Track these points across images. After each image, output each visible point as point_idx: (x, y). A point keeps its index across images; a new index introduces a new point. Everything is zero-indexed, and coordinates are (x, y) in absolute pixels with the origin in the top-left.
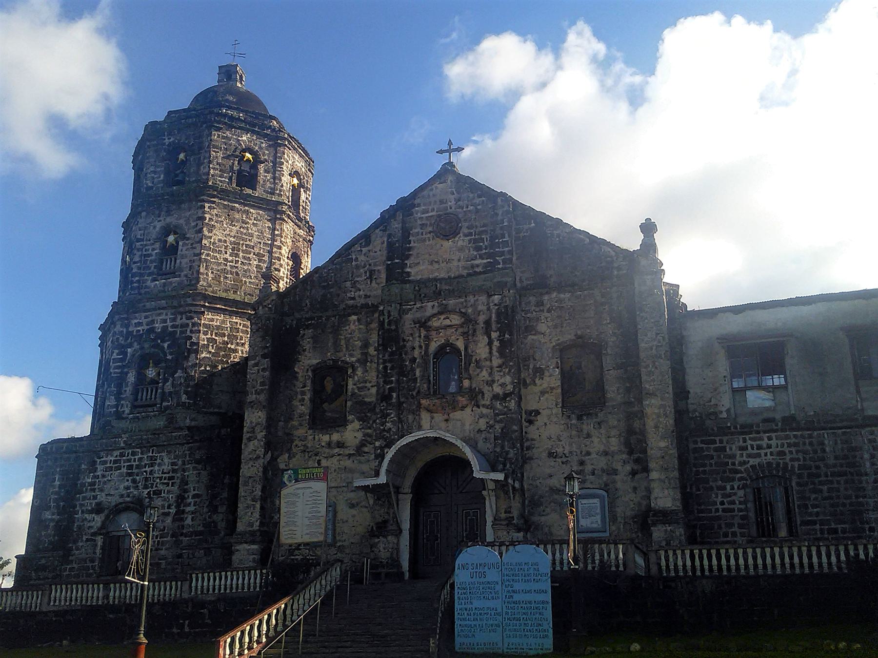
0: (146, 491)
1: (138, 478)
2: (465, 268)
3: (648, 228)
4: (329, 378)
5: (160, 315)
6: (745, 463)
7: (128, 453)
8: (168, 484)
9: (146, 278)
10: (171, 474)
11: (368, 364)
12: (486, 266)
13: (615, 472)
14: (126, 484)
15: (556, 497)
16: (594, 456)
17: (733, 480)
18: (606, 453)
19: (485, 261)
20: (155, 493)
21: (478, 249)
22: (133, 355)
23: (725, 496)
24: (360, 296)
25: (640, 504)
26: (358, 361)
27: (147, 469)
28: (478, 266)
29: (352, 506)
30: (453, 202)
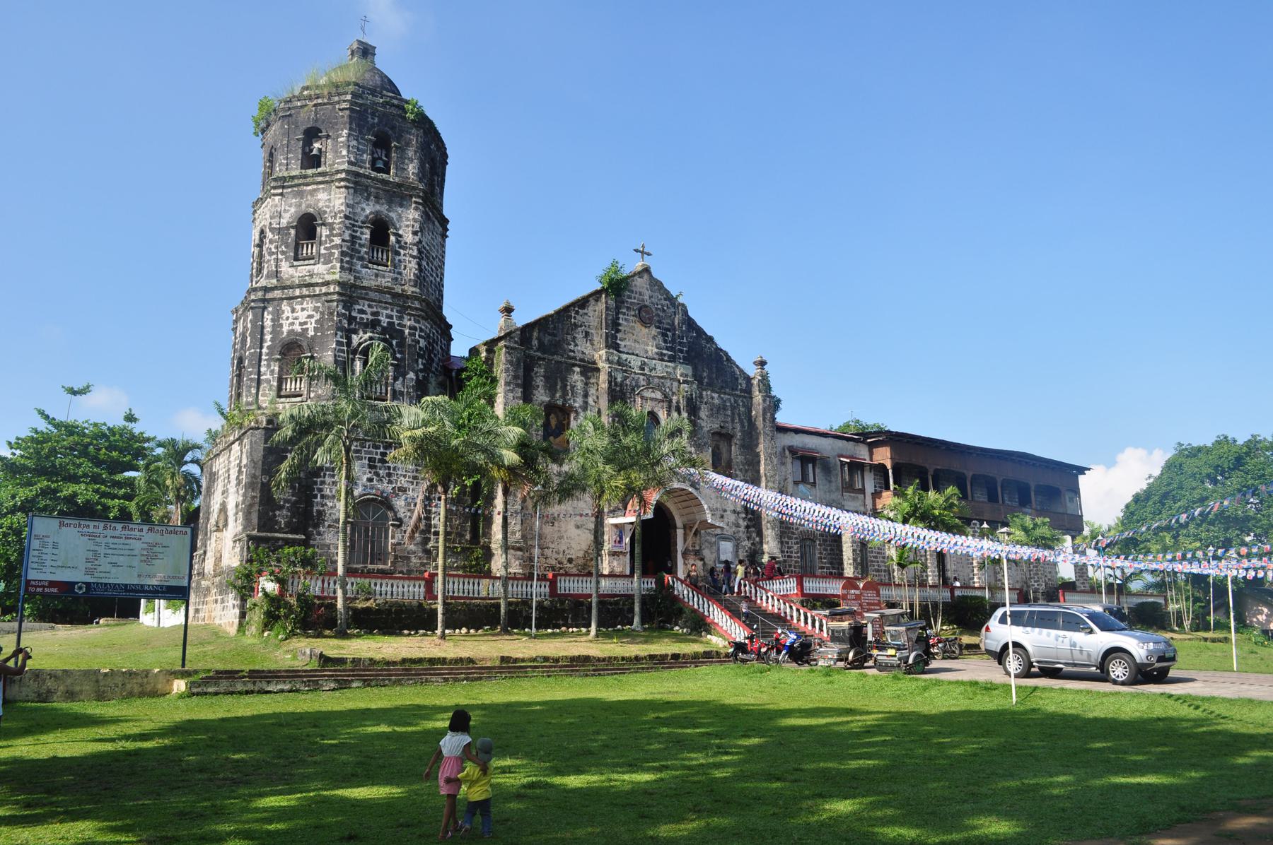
0: (390, 487)
1: (381, 472)
2: (657, 353)
3: (762, 363)
4: (552, 415)
5: (386, 308)
6: (797, 529)
7: (369, 445)
8: (412, 483)
9: (355, 261)
10: (415, 474)
11: (589, 411)
12: (670, 356)
13: (738, 526)
14: (369, 475)
15: (708, 538)
16: (728, 513)
17: (790, 538)
18: (734, 512)
19: (670, 353)
20: (400, 489)
21: (665, 341)
22: (360, 344)
23: (789, 548)
24: (578, 351)
25: (750, 548)
26: (580, 407)
27: (390, 465)
28: (665, 355)
29: (578, 527)
30: (648, 298)
